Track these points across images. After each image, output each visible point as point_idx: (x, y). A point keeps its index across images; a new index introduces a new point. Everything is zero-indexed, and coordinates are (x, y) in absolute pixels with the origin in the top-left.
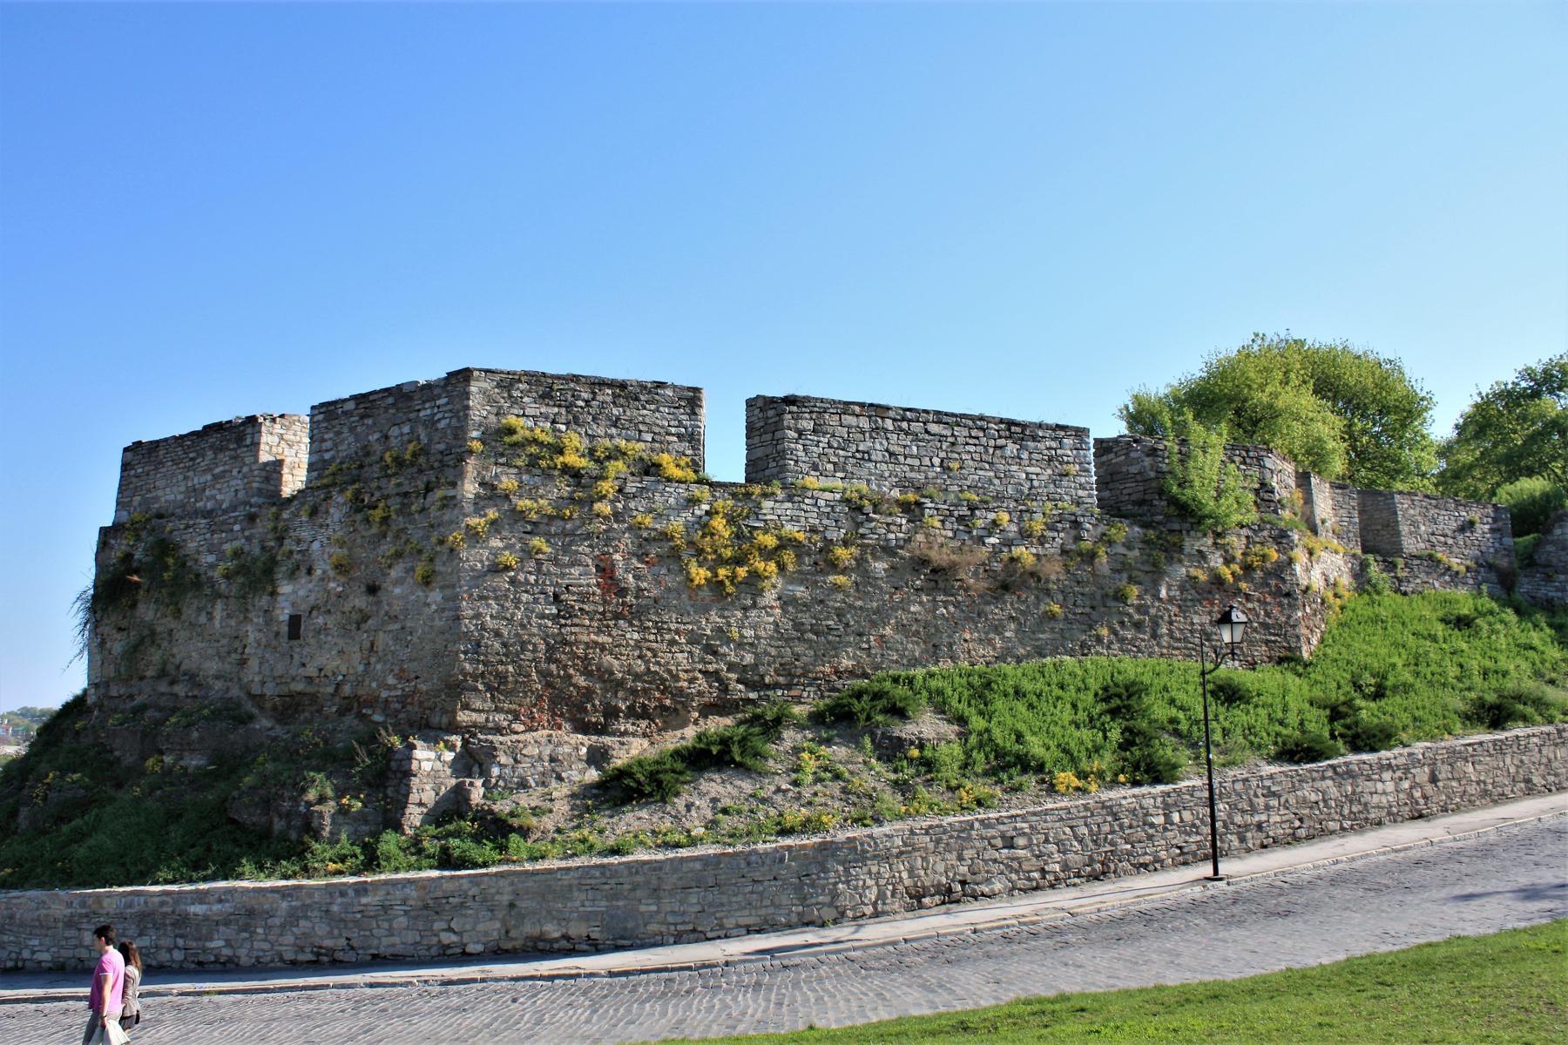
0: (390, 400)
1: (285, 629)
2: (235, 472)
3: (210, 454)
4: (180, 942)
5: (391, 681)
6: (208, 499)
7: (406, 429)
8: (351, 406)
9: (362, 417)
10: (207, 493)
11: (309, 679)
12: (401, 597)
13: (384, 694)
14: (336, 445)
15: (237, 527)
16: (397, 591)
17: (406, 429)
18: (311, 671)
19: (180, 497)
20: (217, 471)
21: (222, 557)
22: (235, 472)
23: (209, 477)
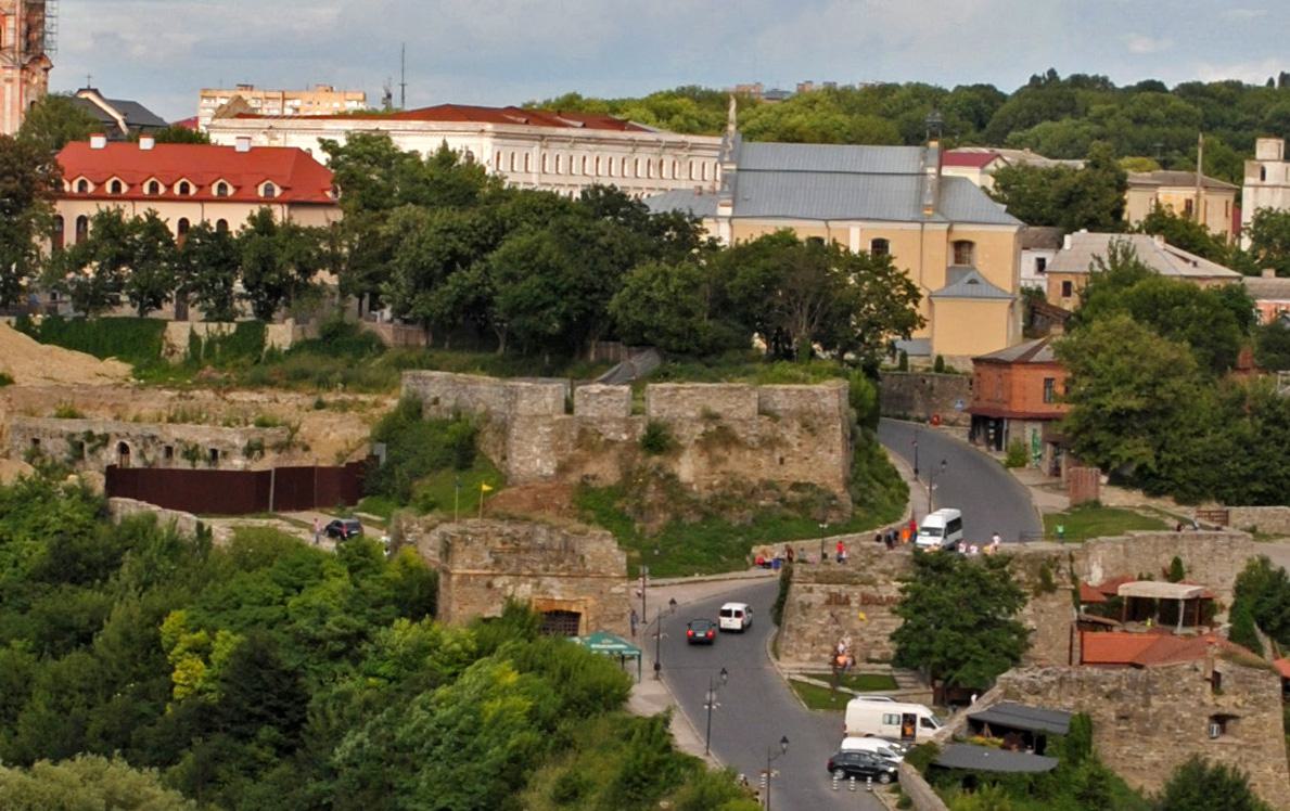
3: (734, 399)
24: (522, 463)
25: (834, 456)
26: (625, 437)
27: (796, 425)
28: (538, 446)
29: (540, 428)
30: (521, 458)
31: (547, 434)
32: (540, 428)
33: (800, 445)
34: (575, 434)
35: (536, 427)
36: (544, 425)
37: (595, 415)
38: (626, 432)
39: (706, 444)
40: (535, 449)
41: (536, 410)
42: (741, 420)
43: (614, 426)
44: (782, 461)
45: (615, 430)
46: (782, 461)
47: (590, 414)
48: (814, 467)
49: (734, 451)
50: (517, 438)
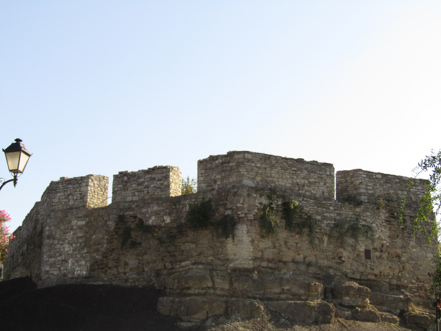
0: (397, 180)
1: (363, 254)
2: (322, 184)
3: (305, 172)
5: (413, 281)
8: (380, 176)
9: (386, 183)
10: (306, 188)
11: (376, 275)
13: (410, 285)
14: (373, 189)
15: (331, 208)
18: (376, 272)
19: (289, 185)
21: (325, 218)
23: (306, 182)
24: (52, 265)
26: (168, 220)
28: (70, 244)
29: (74, 222)
31: (80, 228)
32: (74, 222)
34: (112, 224)
35: (70, 222)
36: (78, 218)
37: (135, 198)
38: (170, 214)
40: (67, 248)
41: (71, 203)
42: (315, 198)
43: (156, 208)
45: (156, 213)
46: (368, 254)
47: (129, 199)
48: (407, 266)
50: (49, 237)
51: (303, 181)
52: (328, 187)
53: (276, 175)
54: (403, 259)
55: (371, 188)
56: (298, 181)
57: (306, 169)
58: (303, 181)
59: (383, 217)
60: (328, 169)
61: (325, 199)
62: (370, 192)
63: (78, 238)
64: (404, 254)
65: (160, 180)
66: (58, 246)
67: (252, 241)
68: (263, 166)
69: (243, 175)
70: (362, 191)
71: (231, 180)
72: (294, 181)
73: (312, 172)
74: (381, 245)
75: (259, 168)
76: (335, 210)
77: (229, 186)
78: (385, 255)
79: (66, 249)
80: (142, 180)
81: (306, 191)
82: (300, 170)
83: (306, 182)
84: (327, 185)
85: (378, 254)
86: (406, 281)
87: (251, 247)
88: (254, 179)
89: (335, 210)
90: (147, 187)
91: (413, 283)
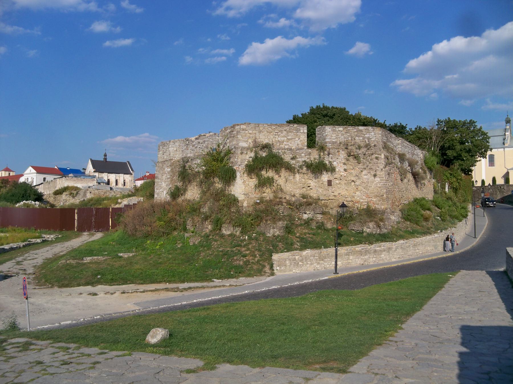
1: (326, 183)
2: (297, 139)
3: (285, 132)
4: (375, 256)
5: (364, 198)
6: (286, 145)
7: (361, 138)
10: (285, 143)
12: (365, 179)
13: (362, 201)
15: (303, 155)
16: (365, 177)
17: (361, 138)
18: (336, 194)
20: (289, 137)
22: (297, 139)
25: (377, 179)
27: (343, 154)
30: (158, 191)
32: (166, 169)
33: (345, 170)
39: (253, 169)
41: (165, 157)
44: (330, 183)
46: (330, 183)
48: (360, 188)
49: (284, 173)
51: (282, 139)
52: (301, 141)
53: (264, 137)
54: (357, 183)
55: (334, 138)
56: (279, 139)
57: (285, 131)
58: (282, 139)
59: (342, 157)
60: (302, 129)
61: (298, 149)
62: (334, 140)
63: (168, 178)
64: (358, 180)
65: (202, 143)
66: (160, 183)
67: (244, 182)
68: (254, 132)
69: (239, 140)
70: (327, 140)
71: (234, 143)
72: (277, 139)
73: (290, 132)
74: (340, 176)
75: (250, 134)
76: (305, 156)
77: (233, 147)
78: (343, 182)
79: (163, 185)
80: (194, 143)
81: (286, 145)
82: (281, 131)
83: (285, 139)
84: (301, 139)
85: (337, 182)
86: (358, 198)
87: (243, 186)
88: (247, 141)
89: (305, 156)
90: (196, 148)
91: (363, 199)
